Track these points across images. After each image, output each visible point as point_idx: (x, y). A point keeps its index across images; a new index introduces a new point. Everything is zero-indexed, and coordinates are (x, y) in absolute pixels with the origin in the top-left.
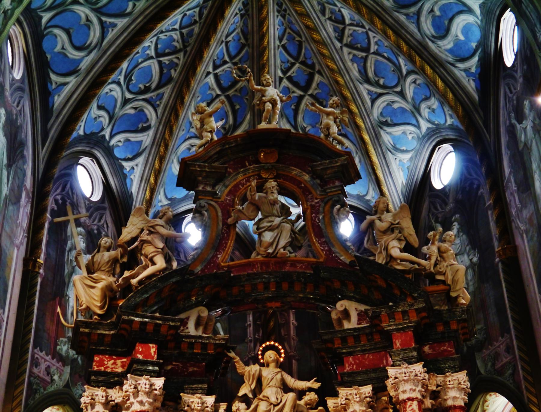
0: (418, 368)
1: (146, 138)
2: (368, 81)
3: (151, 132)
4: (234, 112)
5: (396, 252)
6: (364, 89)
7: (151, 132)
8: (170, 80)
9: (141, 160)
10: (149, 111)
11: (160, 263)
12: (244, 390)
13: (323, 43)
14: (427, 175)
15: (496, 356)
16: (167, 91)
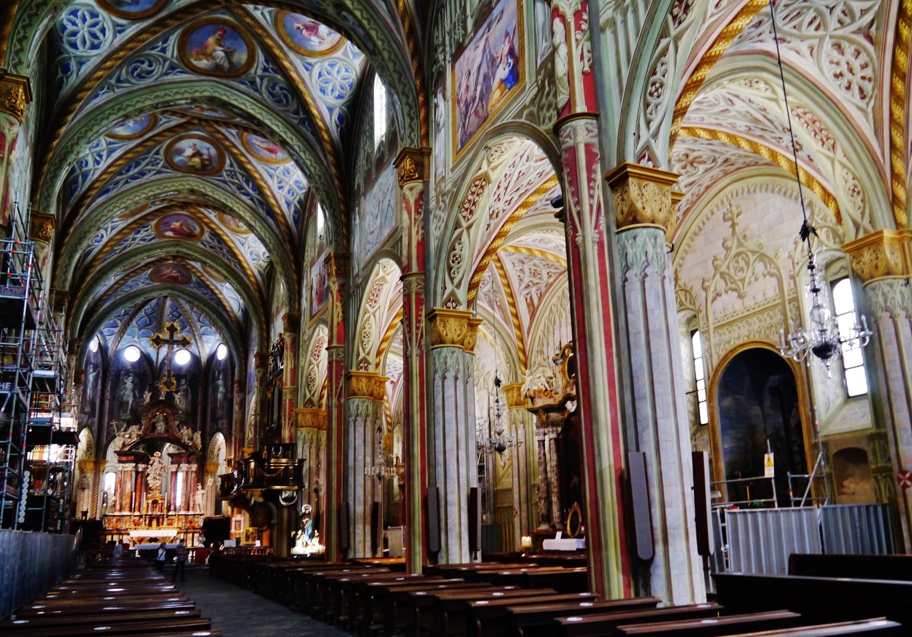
0: (187, 465)
1: (116, 330)
2: (199, 321)
3: (118, 328)
4: (150, 321)
5: (186, 441)
6: (198, 324)
7: (118, 328)
8: (128, 314)
9: (113, 336)
10: (119, 323)
11: (135, 439)
12: (151, 462)
13: (185, 311)
14: (215, 352)
15: (223, 424)
16: (126, 317)
